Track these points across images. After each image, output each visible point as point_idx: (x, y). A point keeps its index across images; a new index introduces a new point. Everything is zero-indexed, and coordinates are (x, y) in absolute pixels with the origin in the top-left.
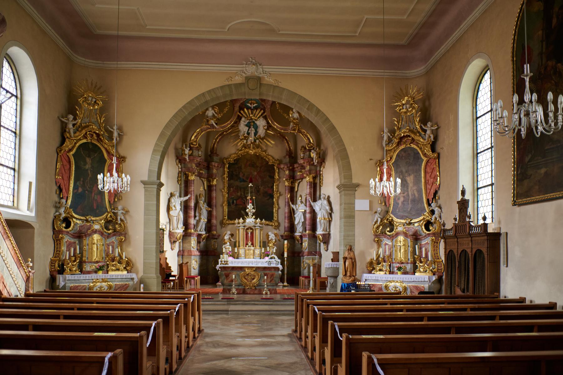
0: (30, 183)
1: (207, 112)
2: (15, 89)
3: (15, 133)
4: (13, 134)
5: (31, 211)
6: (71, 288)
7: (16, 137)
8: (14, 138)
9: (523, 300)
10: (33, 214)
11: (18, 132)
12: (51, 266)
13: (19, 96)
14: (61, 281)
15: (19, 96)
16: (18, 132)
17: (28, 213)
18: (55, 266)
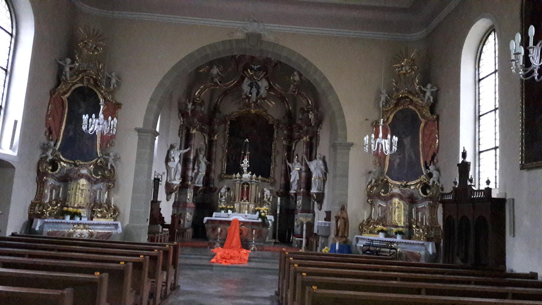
0: (16, 122)
1: (212, 70)
2: (11, 28)
3: (6, 71)
4: (4, 72)
5: (14, 151)
6: (48, 233)
7: (6, 75)
8: (5, 75)
9: (534, 276)
10: (15, 154)
11: (9, 70)
12: (31, 209)
13: (14, 34)
14: (38, 224)
15: (14, 34)
16: (9, 70)
17: (10, 152)
18: (34, 209)
